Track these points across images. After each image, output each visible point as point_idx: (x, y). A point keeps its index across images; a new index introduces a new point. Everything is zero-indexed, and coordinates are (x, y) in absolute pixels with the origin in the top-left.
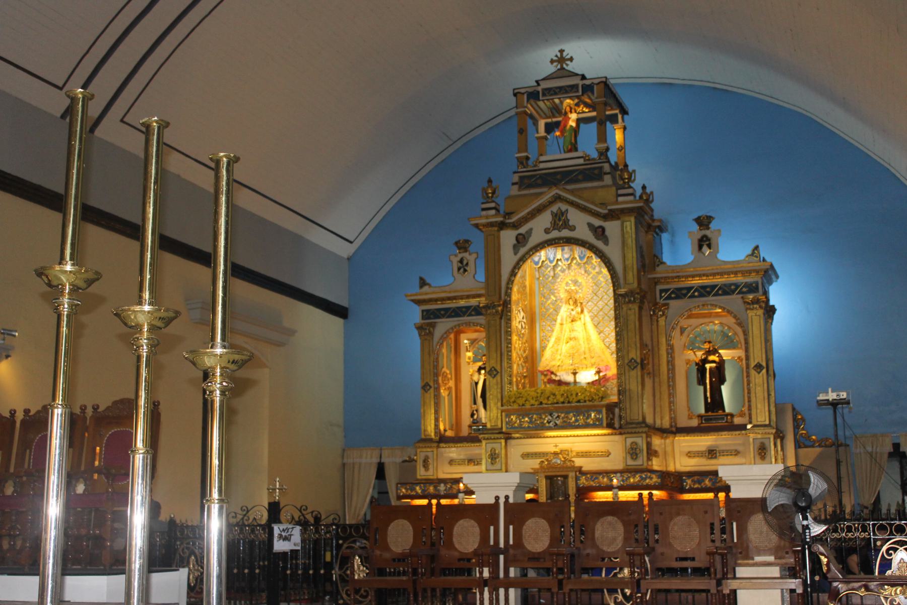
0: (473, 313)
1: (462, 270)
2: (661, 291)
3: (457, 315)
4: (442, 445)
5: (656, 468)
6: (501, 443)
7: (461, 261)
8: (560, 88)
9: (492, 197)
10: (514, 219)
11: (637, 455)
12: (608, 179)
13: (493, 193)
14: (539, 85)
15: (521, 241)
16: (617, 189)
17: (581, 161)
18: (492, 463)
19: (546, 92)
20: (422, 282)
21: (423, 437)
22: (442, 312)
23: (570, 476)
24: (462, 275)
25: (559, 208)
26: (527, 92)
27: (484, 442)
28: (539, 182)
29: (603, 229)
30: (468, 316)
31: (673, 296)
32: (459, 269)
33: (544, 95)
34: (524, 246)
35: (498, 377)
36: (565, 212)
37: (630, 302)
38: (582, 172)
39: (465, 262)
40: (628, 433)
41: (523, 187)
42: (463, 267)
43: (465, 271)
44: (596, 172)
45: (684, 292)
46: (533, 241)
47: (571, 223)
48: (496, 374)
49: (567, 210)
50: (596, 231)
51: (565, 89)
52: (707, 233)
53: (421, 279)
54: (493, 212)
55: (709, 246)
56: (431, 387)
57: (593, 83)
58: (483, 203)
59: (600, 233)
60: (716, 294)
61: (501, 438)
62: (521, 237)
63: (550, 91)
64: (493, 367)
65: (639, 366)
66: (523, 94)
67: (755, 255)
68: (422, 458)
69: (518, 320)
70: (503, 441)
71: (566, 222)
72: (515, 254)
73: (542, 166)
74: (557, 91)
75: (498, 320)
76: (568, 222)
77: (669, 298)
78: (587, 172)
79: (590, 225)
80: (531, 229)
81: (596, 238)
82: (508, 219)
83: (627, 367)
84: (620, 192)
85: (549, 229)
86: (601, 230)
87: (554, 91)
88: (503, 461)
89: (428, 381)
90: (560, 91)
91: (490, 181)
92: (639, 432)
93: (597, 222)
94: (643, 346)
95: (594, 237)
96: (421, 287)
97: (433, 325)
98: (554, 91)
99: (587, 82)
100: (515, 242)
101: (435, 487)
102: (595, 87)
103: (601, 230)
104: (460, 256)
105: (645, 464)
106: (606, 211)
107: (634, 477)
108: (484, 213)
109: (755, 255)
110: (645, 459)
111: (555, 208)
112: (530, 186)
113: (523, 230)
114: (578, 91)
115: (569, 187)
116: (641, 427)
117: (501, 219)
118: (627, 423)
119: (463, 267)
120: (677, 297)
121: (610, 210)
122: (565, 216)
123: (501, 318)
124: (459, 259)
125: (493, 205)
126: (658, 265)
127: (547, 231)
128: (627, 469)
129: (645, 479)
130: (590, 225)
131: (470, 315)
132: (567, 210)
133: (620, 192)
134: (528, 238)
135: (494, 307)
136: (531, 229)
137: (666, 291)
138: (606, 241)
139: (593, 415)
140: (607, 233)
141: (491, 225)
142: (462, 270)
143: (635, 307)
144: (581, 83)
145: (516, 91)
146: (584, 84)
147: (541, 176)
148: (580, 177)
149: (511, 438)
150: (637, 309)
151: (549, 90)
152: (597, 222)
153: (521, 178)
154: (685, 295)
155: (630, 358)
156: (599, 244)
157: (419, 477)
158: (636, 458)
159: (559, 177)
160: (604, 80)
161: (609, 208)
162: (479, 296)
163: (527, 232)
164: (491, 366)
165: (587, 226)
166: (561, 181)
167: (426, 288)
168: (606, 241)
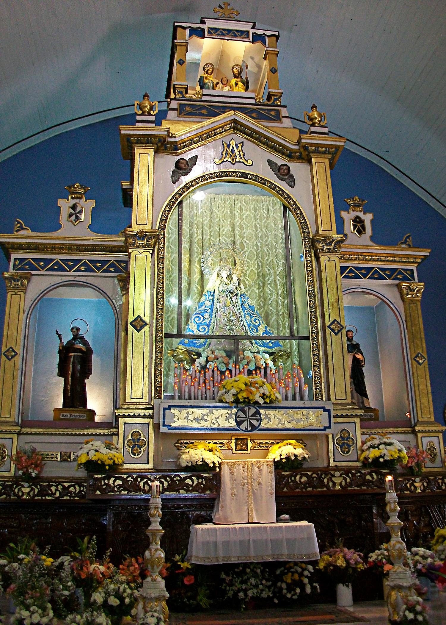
0: (83, 268)
1: (73, 217)
7: (74, 207)
8: (229, 31)
11: (349, 446)
14: (203, 22)
15: (183, 166)
17: (253, 101)
18: (134, 454)
22: (42, 264)
26: (190, 27)
32: (70, 216)
33: (209, 33)
34: (186, 174)
36: (240, 143)
39: (78, 210)
43: (77, 218)
44: (273, 113)
46: (196, 172)
57: (264, 34)
63: (216, 32)
66: (185, 28)
67: (407, 243)
73: (205, 98)
75: (149, 256)
79: (270, 162)
80: (196, 157)
84: (313, 129)
86: (285, 167)
87: (221, 32)
90: (228, 34)
93: (280, 160)
99: (259, 32)
100: (173, 167)
102: (266, 38)
104: (71, 202)
109: (407, 243)
114: (248, 37)
119: (76, 213)
124: (71, 205)
130: (270, 162)
131: (78, 270)
132: (243, 142)
136: (196, 157)
142: (73, 217)
144: (252, 31)
145: (176, 24)
146: (255, 33)
147: (203, 107)
152: (280, 160)
156: (283, 185)
160: (277, 34)
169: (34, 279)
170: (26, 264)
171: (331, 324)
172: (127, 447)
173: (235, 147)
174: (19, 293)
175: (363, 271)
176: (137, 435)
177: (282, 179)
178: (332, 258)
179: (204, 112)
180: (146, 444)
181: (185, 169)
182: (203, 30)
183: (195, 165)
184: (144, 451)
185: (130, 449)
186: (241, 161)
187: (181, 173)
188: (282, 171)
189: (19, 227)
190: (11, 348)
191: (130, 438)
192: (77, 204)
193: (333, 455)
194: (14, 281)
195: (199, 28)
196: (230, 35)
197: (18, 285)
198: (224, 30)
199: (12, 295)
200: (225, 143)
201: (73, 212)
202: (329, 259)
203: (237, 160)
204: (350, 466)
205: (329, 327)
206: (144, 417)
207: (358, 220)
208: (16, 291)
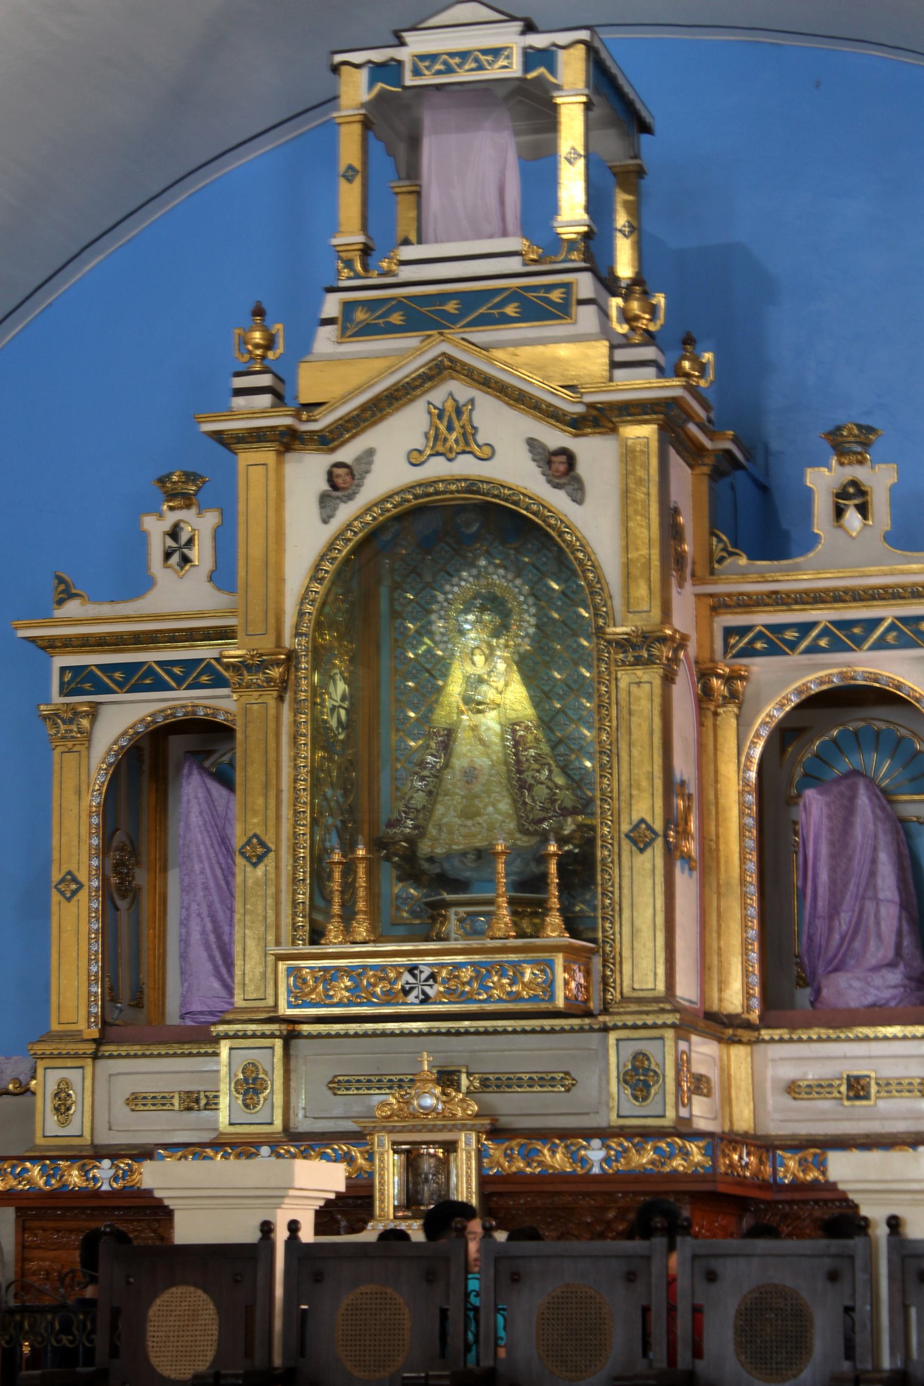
0: (204, 679)
1: (175, 558)
2: (729, 632)
3: (160, 686)
4: (107, 1049)
5: (701, 1125)
6: (272, 1048)
7: (174, 533)
9: (264, 357)
10: (323, 421)
11: (647, 1086)
12: (587, 317)
13: (269, 344)
15: (339, 481)
16: (612, 347)
18: (247, 1106)
19: (422, 65)
20: (62, 587)
21: (55, 1027)
23: (462, 1145)
24: (176, 572)
25: (451, 394)
26: (370, 62)
27: (224, 1048)
28: (396, 318)
29: (569, 457)
30: (189, 687)
31: (759, 645)
32: (168, 555)
34: (350, 498)
35: (271, 858)
37: (638, 662)
38: (515, 295)
39: (184, 538)
40: (625, 1027)
41: (349, 333)
42: (180, 548)
43: (185, 560)
45: (790, 635)
47: (481, 439)
48: (265, 854)
49: (472, 401)
50: (549, 463)
51: (477, 60)
52: (860, 473)
53: (61, 580)
54: (265, 400)
55: (863, 510)
56: (80, 886)
57: (555, 45)
58: (238, 374)
59: (562, 468)
60: (881, 645)
61: (273, 1036)
62: (341, 471)
64: (255, 836)
65: (659, 843)
68: (52, 1088)
69: (329, 704)
70: (278, 1043)
71: (469, 436)
72: (325, 521)
73: (407, 273)
74: (453, 62)
75: (272, 703)
76: (474, 435)
77: (749, 652)
78: (530, 295)
79: (532, 444)
80: (370, 452)
81: (549, 482)
82: (308, 421)
83: (626, 845)
84: (622, 355)
85: (420, 452)
86: (563, 458)
87: (445, 63)
88: (278, 1099)
89: (73, 868)
91: (259, 312)
92: (655, 1026)
94: (671, 787)
95: (543, 479)
96: (60, 602)
97: (94, 713)
98: (445, 63)
100: (325, 487)
101: (84, 1172)
103: (563, 458)
104: (171, 518)
105: (671, 1113)
106: (580, 409)
107: (640, 1150)
108: (240, 402)
110: (670, 1099)
111: (438, 396)
112: (368, 331)
113: (347, 454)
115: (481, 336)
116: (663, 1011)
117: (288, 421)
118: (625, 999)
119: (180, 548)
120: (773, 650)
121: (591, 406)
122: (465, 417)
123: (281, 699)
124: (167, 525)
125: (265, 380)
126: (721, 560)
127: (415, 459)
128: (622, 1128)
129: (671, 1156)
130: (532, 444)
132: (472, 401)
133: (622, 355)
134: (362, 478)
135: (263, 666)
136: (370, 452)
137: (742, 631)
138: (577, 492)
139: (528, 972)
140: (582, 469)
141: (257, 437)
142: (175, 558)
143: (652, 676)
145: (338, 58)
146: (531, 47)
147: (399, 304)
148: (510, 310)
149: (298, 1035)
150: (657, 682)
151: (433, 58)
153: (348, 307)
154: (793, 645)
155: (635, 818)
156: (558, 500)
157: (39, 1140)
158: (645, 1099)
159: (451, 307)
161: (588, 399)
162: (225, 634)
163: (358, 460)
164: (251, 834)
165: (526, 447)
166: (453, 319)
167: (72, 608)
168: (577, 492)
169: (106, 713)
170: (82, 682)
171: (632, 831)
172: (234, 1093)
173: (454, 416)
174: (75, 749)
175: (857, 630)
176: (252, 1072)
177: (557, 486)
178: (646, 678)
179: (396, 318)
180: (269, 1087)
181: (344, 489)
182: (400, 63)
183: (368, 472)
184: (265, 1099)
185: (241, 1097)
186: (468, 449)
187: (338, 498)
188: (555, 466)
189: (62, 592)
190: (69, 873)
191: (241, 1076)
192: (182, 525)
193: (616, 1104)
194: (64, 722)
195: (393, 59)
196: (467, 67)
197: (71, 731)
198: (452, 55)
199: (62, 753)
200: (435, 408)
201: (174, 545)
202: (638, 680)
203: (459, 449)
204: (650, 1127)
205: (627, 836)
206: (264, 1036)
207: (851, 490)
208: (70, 744)
